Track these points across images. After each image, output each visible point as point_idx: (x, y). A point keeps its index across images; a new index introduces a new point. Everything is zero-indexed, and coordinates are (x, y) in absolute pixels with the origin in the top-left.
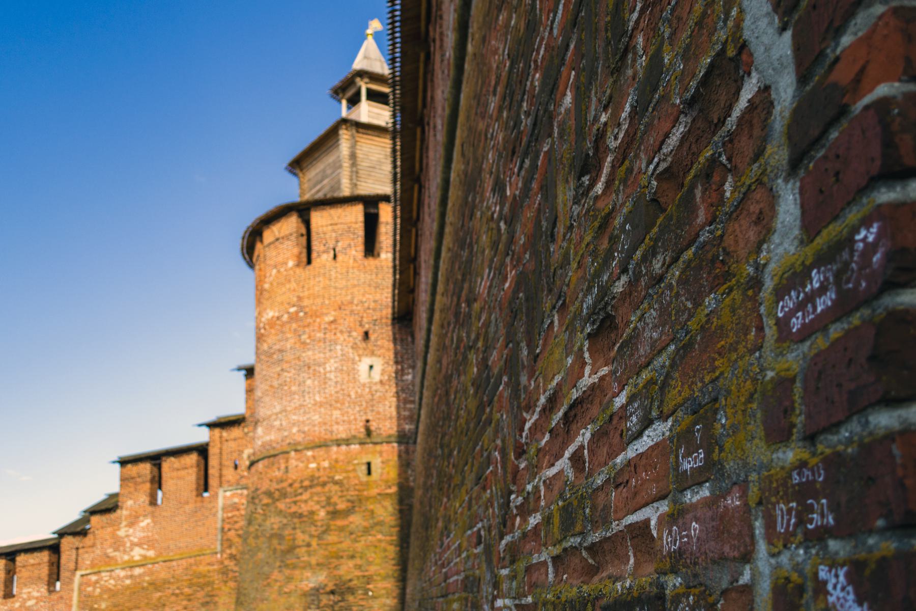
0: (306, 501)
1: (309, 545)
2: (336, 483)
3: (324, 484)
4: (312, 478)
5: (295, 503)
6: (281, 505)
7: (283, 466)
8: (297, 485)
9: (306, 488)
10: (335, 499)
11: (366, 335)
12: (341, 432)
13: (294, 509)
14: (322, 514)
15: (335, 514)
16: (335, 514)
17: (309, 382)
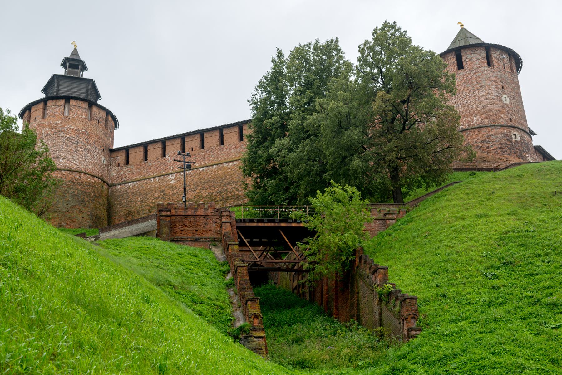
0: (87, 189)
1: (89, 202)
2: (96, 188)
3: (93, 187)
4: (89, 183)
5: (84, 188)
6: (78, 187)
7: (78, 176)
8: (84, 183)
9: (87, 185)
10: (96, 192)
11: (104, 149)
12: (96, 174)
13: (83, 190)
14: (93, 194)
15: (96, 196)
16: (96, 196)
17: (88, 155)
